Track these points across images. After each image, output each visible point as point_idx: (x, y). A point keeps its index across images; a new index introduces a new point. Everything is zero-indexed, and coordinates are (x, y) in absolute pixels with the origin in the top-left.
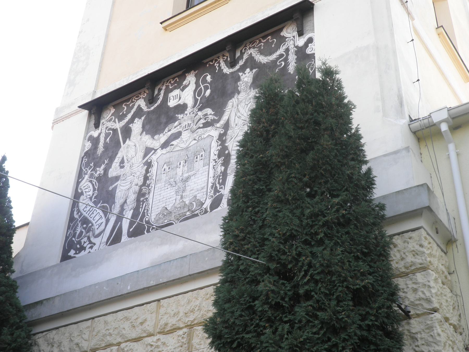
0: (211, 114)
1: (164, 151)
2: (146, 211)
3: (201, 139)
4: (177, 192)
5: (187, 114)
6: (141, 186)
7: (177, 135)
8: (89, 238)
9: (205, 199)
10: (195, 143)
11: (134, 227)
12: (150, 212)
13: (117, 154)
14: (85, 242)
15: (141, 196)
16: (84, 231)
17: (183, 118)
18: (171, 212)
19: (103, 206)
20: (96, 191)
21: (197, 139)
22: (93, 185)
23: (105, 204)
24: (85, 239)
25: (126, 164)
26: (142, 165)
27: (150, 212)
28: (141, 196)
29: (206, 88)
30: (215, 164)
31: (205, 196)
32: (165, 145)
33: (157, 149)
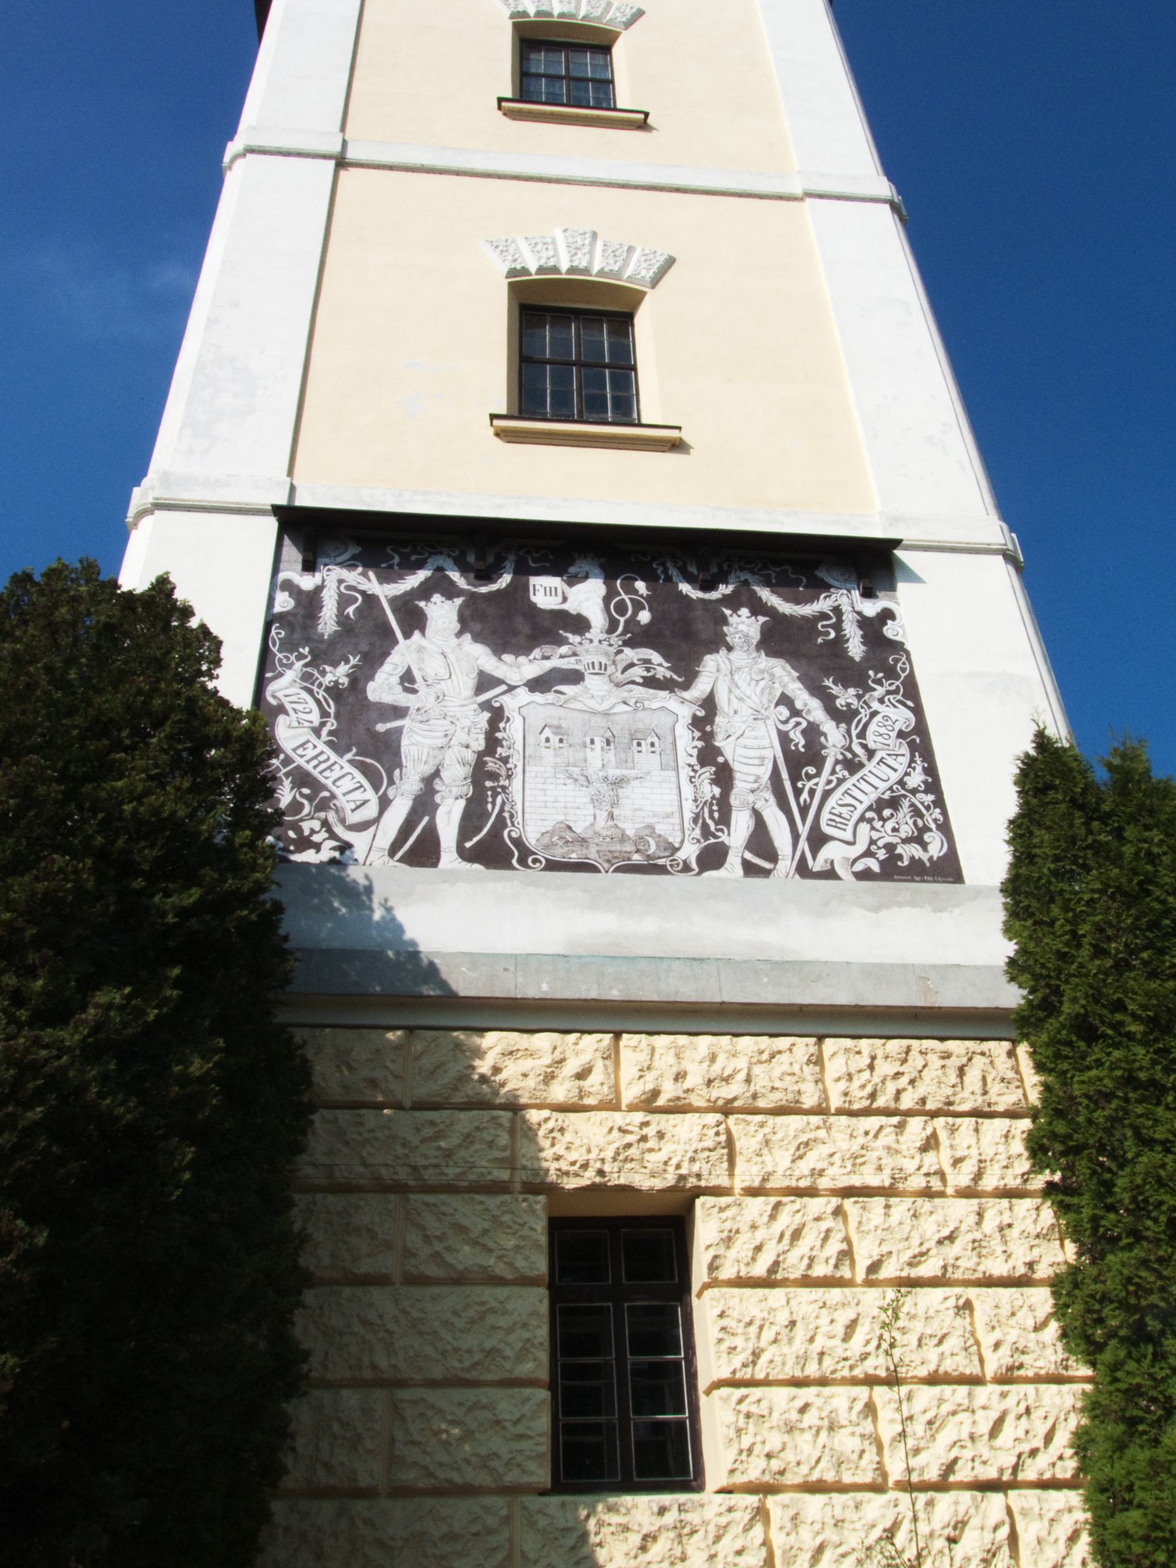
0: (660, 665)
1: (538, 697)
2: (506, 815)
3: (644, 709)
4: (595, 801)
5: (591, 641)
6: (481, 755)
7: (575, 677)
8: (325, 824)
9: (679, 840)
10: (626, 712)
11: (475, 839)
12: (520, 819)
13: (386, 654)
14: (313, 832)
15: (486, 776)
16: (305, 802)
17: (580, 643)
18: (584, 840)
19: (363, 762)
20: (332, 720)
21: (632, 702)
22: (318, 702)
23: (368, 760)
24: (316, 825)
25: (419, 684)
26: (476, 706)
27: (520, 819)
28: (486, 776)
29: (638, 607)
30: (692, 774)
31: (679, 834)
32: (539, 684)
33: (515, 687)
